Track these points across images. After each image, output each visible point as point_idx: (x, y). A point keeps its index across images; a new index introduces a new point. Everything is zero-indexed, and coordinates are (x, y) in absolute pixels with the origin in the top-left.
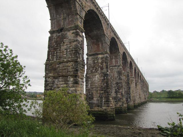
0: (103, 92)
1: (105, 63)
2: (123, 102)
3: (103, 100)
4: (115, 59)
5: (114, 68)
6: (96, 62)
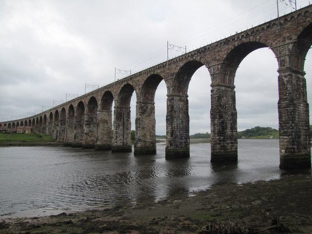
4: (229, 77)
5: (227, 89)
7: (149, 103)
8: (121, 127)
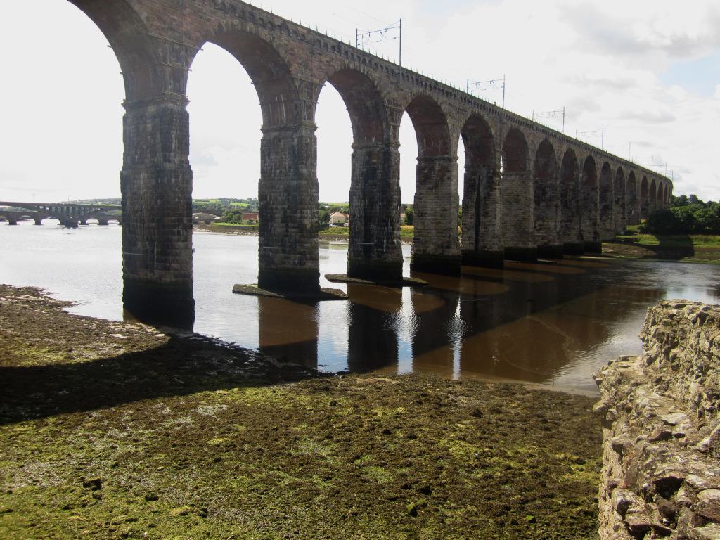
0: (154, 224)
1: (161, 133)
2: (303, 253)
3: (155, 250)
4: (286, 105)
6: (141, 128)
7: (435, 159)
8: (472, 211)
